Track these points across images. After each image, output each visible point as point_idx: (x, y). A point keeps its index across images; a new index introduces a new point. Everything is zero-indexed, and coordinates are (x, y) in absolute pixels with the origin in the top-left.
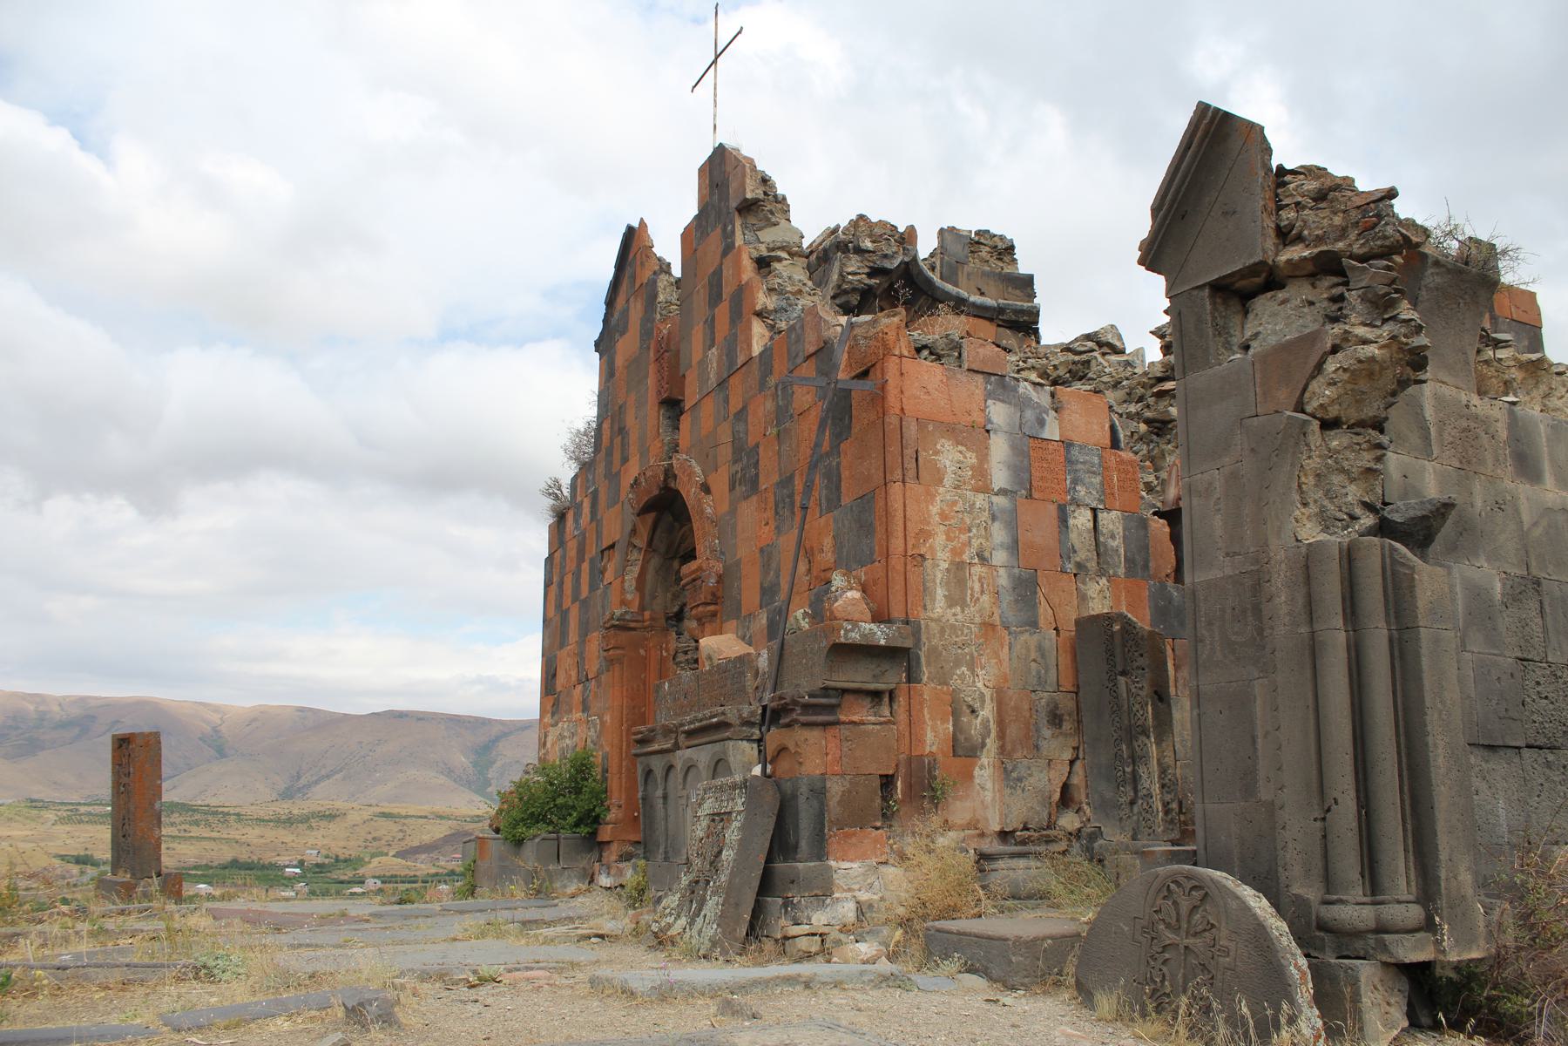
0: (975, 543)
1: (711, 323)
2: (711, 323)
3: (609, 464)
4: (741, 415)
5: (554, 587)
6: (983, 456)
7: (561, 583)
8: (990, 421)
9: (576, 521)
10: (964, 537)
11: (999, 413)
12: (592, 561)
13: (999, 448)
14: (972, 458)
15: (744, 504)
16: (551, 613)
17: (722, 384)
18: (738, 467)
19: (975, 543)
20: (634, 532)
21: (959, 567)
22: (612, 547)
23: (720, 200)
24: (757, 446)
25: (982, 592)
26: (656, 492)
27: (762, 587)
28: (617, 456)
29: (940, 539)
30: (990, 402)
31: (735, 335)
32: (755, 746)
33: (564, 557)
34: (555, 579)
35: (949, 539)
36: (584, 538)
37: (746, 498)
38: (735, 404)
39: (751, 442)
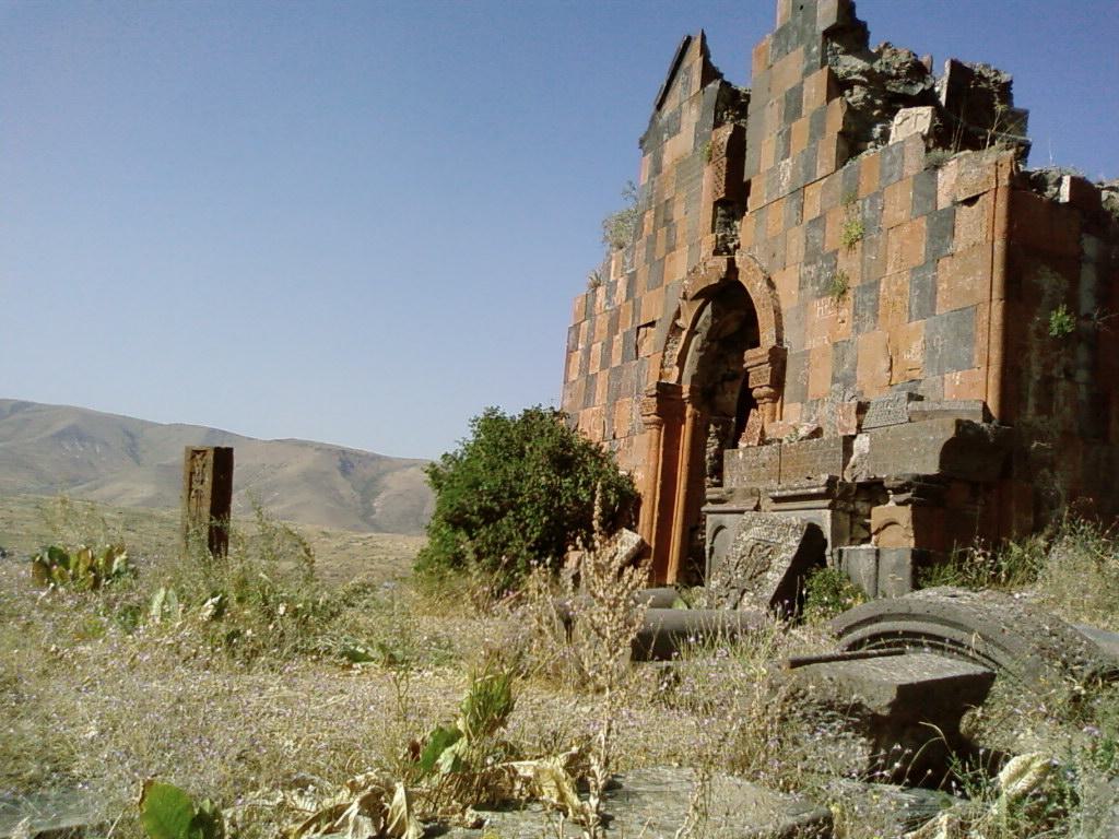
0: (1063, 360)
1: (787, 136)
2: (787, 136)
3: (651, 251)
5: (578, 356)
6: (1075, 282)
7: (588, 351)
8: (1082, 252)
9: (608, 297)
10: (1054, 354)
11: (1090, 246)
12: (625, 334)
13: (1088, 277)
14: (1065, 284)
16: (574, 376)
17: (798, 192)
18: (812, 268)
19: (1063, 360)
20: (678, 315)
21: (1048, 381)
22: (652, 324)
23: (804, 21)
24: (836, 252)
25: (1065, 404)
26: (715, 281)
28: (661, 245)
29: (1034, 355)
30: (1083, 235)
32: (848, 517)
33: (592, 328)
34: (580, 346)
35: (1042, 354)
36: (618, 313)
38: (812, 212)
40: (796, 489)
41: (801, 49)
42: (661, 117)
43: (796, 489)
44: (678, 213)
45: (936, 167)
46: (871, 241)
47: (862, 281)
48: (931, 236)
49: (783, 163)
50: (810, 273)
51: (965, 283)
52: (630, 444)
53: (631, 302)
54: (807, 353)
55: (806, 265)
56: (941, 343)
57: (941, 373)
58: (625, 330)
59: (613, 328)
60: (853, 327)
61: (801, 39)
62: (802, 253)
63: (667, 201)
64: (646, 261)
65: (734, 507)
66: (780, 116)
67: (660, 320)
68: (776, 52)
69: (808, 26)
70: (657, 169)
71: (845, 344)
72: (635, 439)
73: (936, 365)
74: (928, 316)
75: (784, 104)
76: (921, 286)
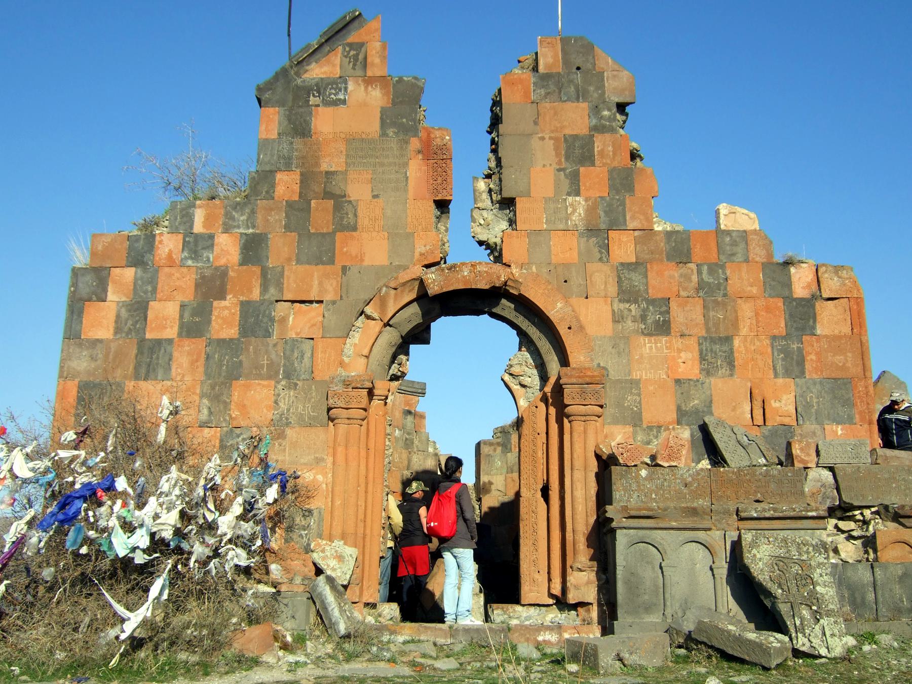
4: (636, 266)
7: (138, 308)
12: (246, 307)
15: (642, 339)
26: (483, 285)
27: (679, 409)
31: (623, 204)
34: (111, 296)
37: (650, 335)
39: (653, 294)
40: (782, 512)
41: (584, 106)
42: (298, 74)
43: (782, 512)
44: (357, 190)
45: (788, 263)
46: (716, 302)
47: (708, 330)
48: (791, 315)
49: (570, 198)
50: (630, 310)
51: (839, 359)
52: (281, 436)
53: (257, 270)
54: (635, 383)
55: (620, 301)
56: (815, 400)
57: (821, 424)
58: (241, 298)
59: (213, 286)
60: (702, 370)
61: (580, 95)
62: (613, 289)
63: (327, 173)
64: (287, 228)
65: (674, 524)
66: (558, 155)
67: (334, 303)
68: (543, 92)
69: (592, 88)
70: (299, 128)
71: (692, 383)
72: (289, 432)
73: (813, 417)
74: (797, 377)
75: (563, 146)
76: (787, 353)
